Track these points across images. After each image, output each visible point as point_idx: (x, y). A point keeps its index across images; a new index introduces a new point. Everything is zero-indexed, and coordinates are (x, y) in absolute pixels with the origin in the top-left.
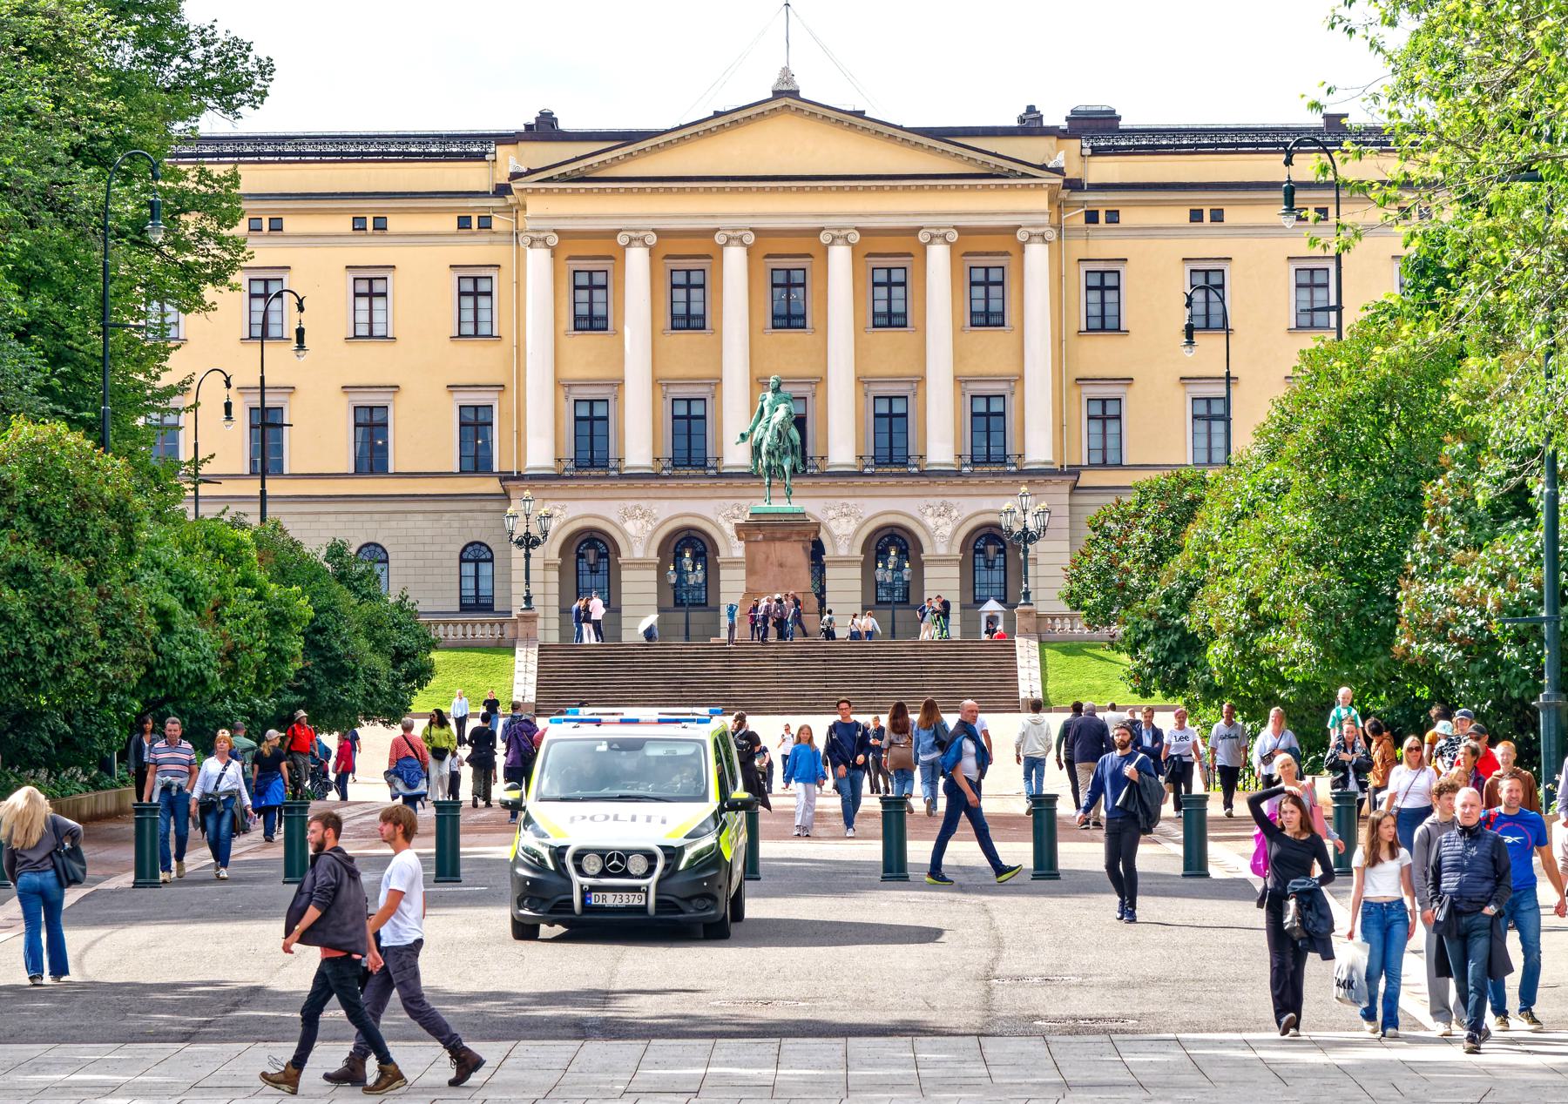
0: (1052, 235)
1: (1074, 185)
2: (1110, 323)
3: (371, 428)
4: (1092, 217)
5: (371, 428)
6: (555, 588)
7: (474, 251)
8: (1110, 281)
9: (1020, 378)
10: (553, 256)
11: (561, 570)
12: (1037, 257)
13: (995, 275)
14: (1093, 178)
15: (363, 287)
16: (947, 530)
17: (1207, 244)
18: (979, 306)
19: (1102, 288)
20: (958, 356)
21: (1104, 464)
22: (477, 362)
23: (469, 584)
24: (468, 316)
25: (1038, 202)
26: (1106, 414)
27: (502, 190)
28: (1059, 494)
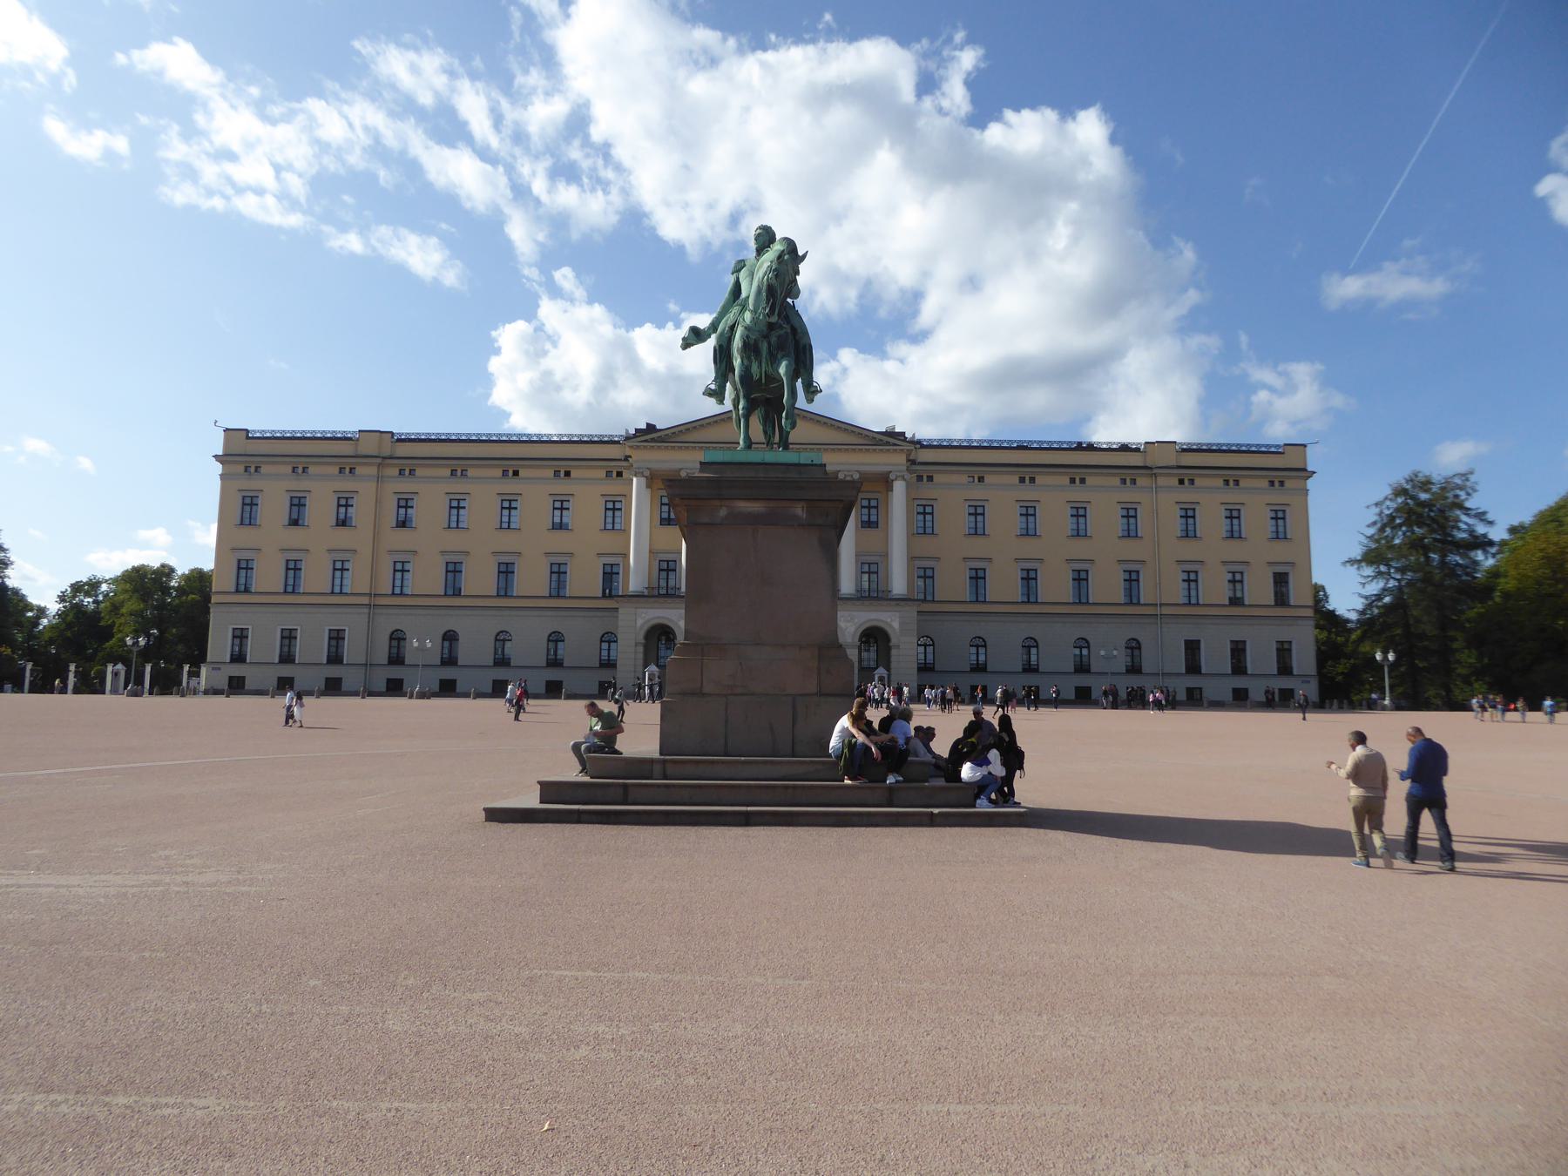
0: (908, 476)
1: (913, 462)
2: (929, 530)
3: (558, 572)
4: (920, 478)
5: (558, 572)
6: (641, 656)
7: (613, 488)
8: (928, 510)
9: (886, 555)
10: (649, 486)
11: (646, 647)
12: (899, 487)
13: (873, 503)
14: (920, 460)
15: (558, 505)
16: (852, 629)
17: (977, 493)
18: (865, 518)
19: (924, 513)
20: (857, 545)
21: (924, 600)
22: (608, 542)
23: (605, 653)
24: (609, 520)
25: (901, 459)
26: (927, 575)
27: (627, 458)
28: (911, 612)
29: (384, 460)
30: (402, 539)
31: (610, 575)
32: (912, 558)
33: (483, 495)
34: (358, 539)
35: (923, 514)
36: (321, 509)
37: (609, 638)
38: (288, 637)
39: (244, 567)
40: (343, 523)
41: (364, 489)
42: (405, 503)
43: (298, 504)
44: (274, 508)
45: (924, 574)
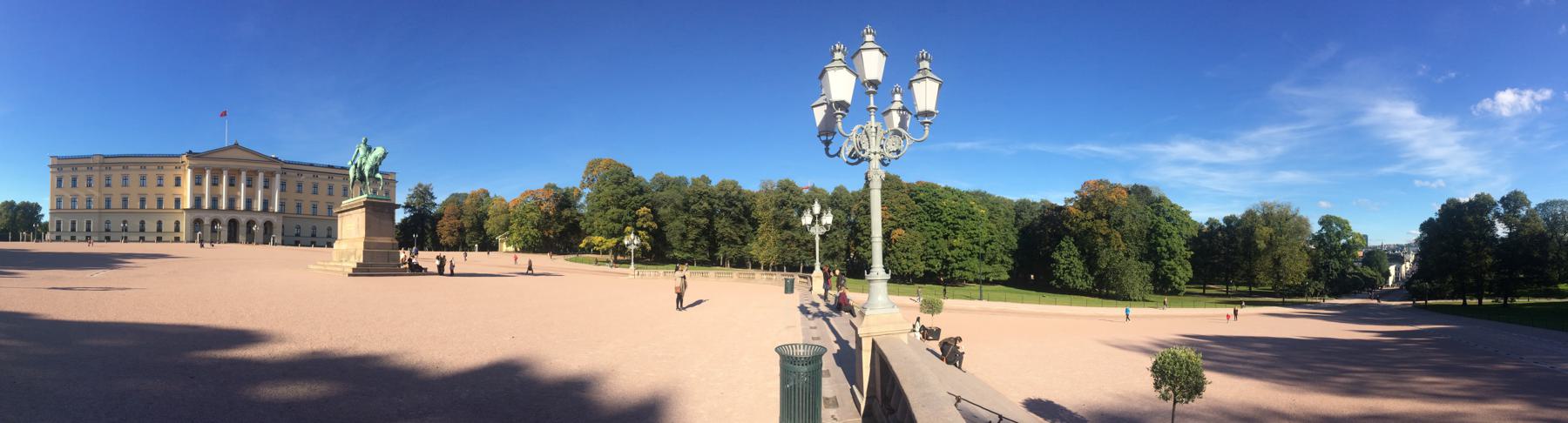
7: (179, 172)
29: (102, 164)
30: (108, 190)
31: (178, 201)
32: (280, 199)
33: (134, 176)
34: (93, 191)
35: (283, 184)
36: (82, 182)
37: (177, 223)
38: (73, 223)
39: (59, 201)
40: (89, 185)
41: (96, 176)
42: (108, 179)
43: (74, 180)
44: (67, 182)
45: (282, 205)
